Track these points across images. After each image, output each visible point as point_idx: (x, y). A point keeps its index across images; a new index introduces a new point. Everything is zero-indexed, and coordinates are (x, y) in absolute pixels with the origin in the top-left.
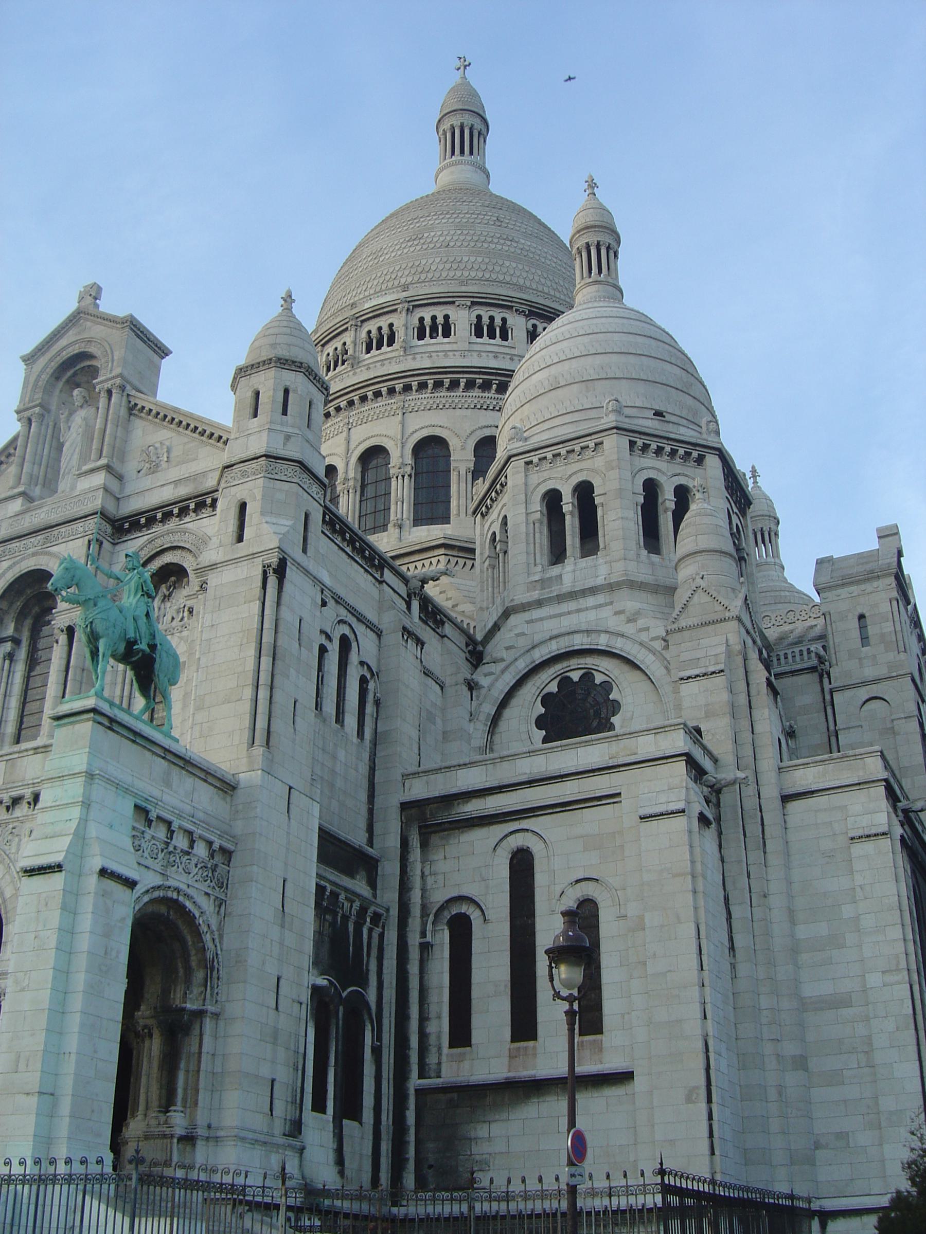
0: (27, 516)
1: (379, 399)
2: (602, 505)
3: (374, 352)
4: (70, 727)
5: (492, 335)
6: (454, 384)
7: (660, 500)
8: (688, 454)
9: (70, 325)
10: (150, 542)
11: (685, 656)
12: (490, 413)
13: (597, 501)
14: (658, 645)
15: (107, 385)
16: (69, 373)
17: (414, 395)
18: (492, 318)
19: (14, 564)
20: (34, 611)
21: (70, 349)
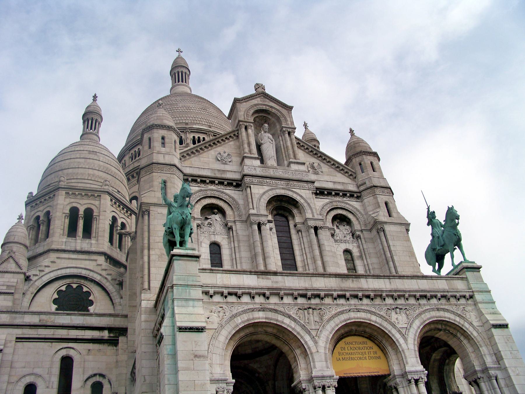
0: (272, 170)
4: (472, 273)
9: (257, 96)
10: (331, 202)
15: (289, 130)
20: (274, 213)
21: (261, 106)
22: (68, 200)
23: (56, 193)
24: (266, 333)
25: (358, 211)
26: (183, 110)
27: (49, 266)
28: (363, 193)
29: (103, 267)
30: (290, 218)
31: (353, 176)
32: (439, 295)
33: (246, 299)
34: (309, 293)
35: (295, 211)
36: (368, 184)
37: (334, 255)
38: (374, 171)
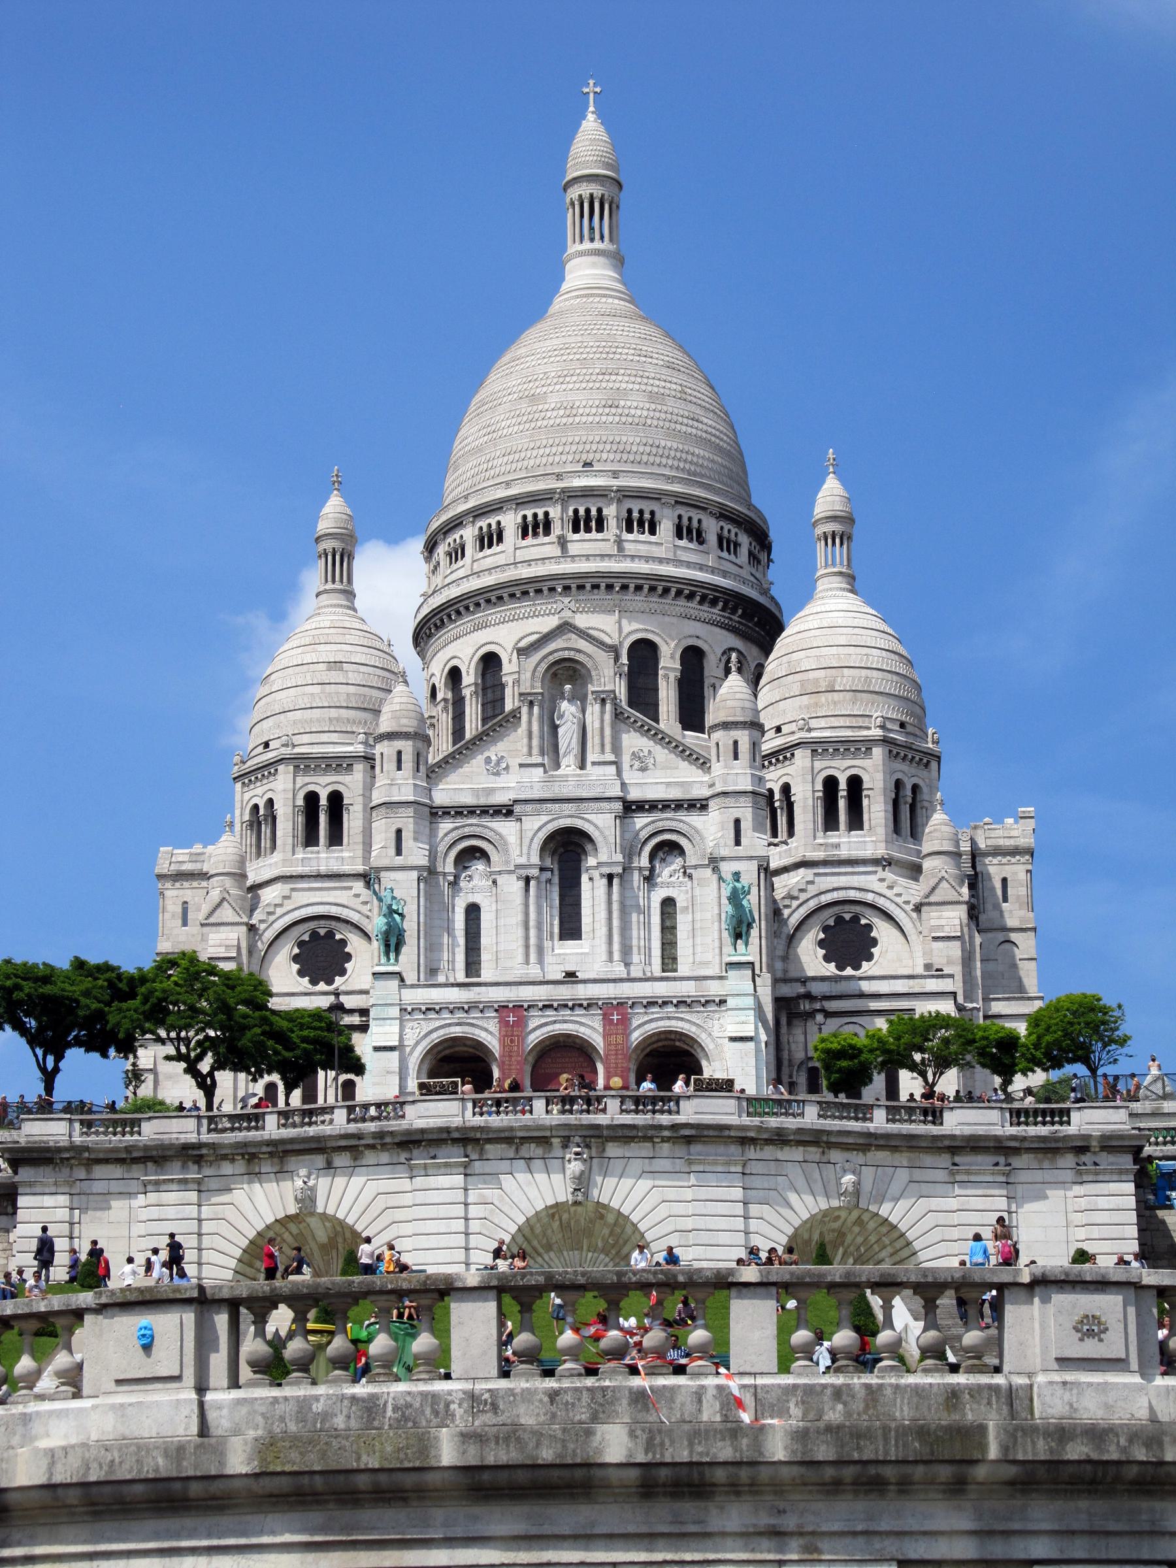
1: (596, 591)
2: (868, 796)
3: (582, 535)
5: (691, 540)
6: (666, 591)
7: (901, 794)
8: (921, 760)
11: (933, 923)
12: (692, 623)
13: (865, 793)
14: (909, 908)
16: (554, 669)
17: (630, 596)
18: (690, 519)
19: (553, 820)
21: (561, 653)
22: (300, 781)
23: (281, 768)
24: (465, 1045)
25: (697, 831)
26: (558, 421)
27: (281, 905)
28: (711, 803)
29: (362, 899)
30: (583, 857)
31: (703, 763)
32: (675, 1001)
33: (446, 1015)
34: (511, 1005)
35: (589, 847)
36: (719, 788)
37: (645, 912)
38: (736, 757)
